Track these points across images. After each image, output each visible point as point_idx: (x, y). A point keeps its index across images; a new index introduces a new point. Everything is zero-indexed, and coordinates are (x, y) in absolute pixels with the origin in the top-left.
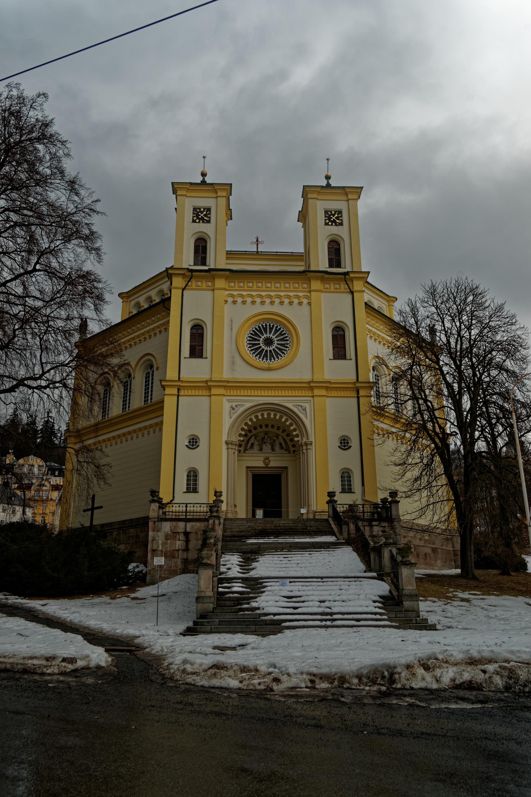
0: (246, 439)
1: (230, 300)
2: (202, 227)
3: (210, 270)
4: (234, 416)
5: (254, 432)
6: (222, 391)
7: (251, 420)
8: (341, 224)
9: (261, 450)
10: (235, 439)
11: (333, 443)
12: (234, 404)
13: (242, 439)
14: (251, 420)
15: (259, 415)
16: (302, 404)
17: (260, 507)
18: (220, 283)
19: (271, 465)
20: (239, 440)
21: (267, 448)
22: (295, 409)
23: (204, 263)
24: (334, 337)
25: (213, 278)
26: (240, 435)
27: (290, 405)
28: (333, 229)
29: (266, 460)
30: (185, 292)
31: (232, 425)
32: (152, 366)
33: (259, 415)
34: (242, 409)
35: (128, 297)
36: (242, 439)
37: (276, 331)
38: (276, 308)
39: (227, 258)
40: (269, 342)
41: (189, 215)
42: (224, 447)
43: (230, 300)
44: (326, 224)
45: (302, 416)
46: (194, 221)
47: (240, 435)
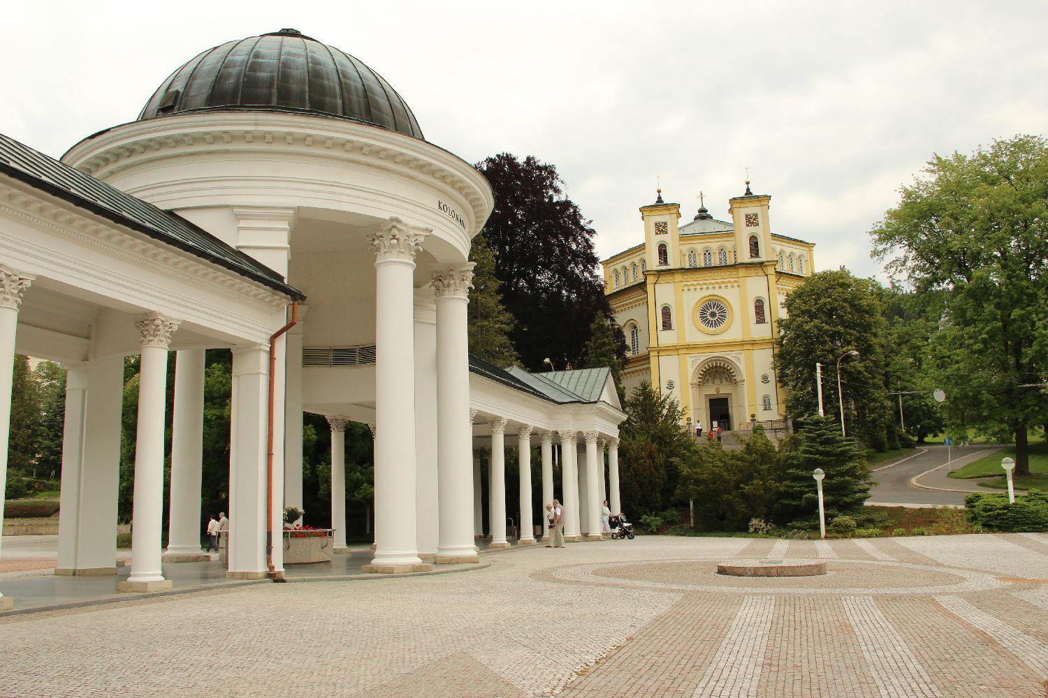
0: (703, 377)
1: (686, 288)
2: (662, 238)
3: (670, 270)
4: (695, 367)
5: (708, 372)
6: (685, 351)
7: (705, 368)
8: (757, 225)
9: (714, 383)
10: (696, 381)
11: (759, 379)
12: (694, 359)
13: (700, 380)
14: (705, 368)
15: (710, 364)
16: (738, 356)
17: (714, 420)
18: (678, 277)
19: (721, 393)
20: (700, 382)
21: (717, 381)
22: (733, 359)
23: (666, 262)
24: (756, 307)
25: (673, 273)
26: (699, 378)
27: (730, 358)
28: (753, 230)
29: (718, 390)
30: (656, 286)
31: (694, 373)
32: (635, 327)
33: (710, 364)
34: (700, 361)
35: (607, 264)
36: (700, 380)
37: (718, 307)
38: (717, 292)
39: (680, 240)
40: (713, 315)
41: (653, 229)
42: (690, 386)
43: (686, 288)
44: (747, 226)
45: (738, 364)
46: (657, 234)
47: (699, 378)
